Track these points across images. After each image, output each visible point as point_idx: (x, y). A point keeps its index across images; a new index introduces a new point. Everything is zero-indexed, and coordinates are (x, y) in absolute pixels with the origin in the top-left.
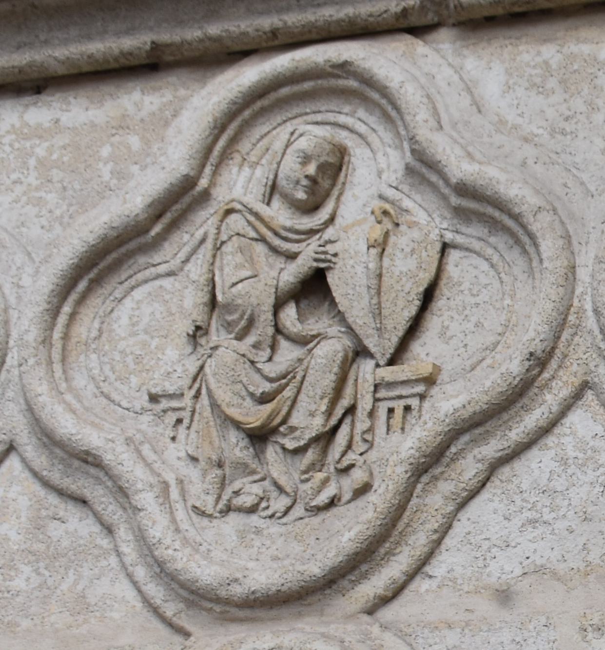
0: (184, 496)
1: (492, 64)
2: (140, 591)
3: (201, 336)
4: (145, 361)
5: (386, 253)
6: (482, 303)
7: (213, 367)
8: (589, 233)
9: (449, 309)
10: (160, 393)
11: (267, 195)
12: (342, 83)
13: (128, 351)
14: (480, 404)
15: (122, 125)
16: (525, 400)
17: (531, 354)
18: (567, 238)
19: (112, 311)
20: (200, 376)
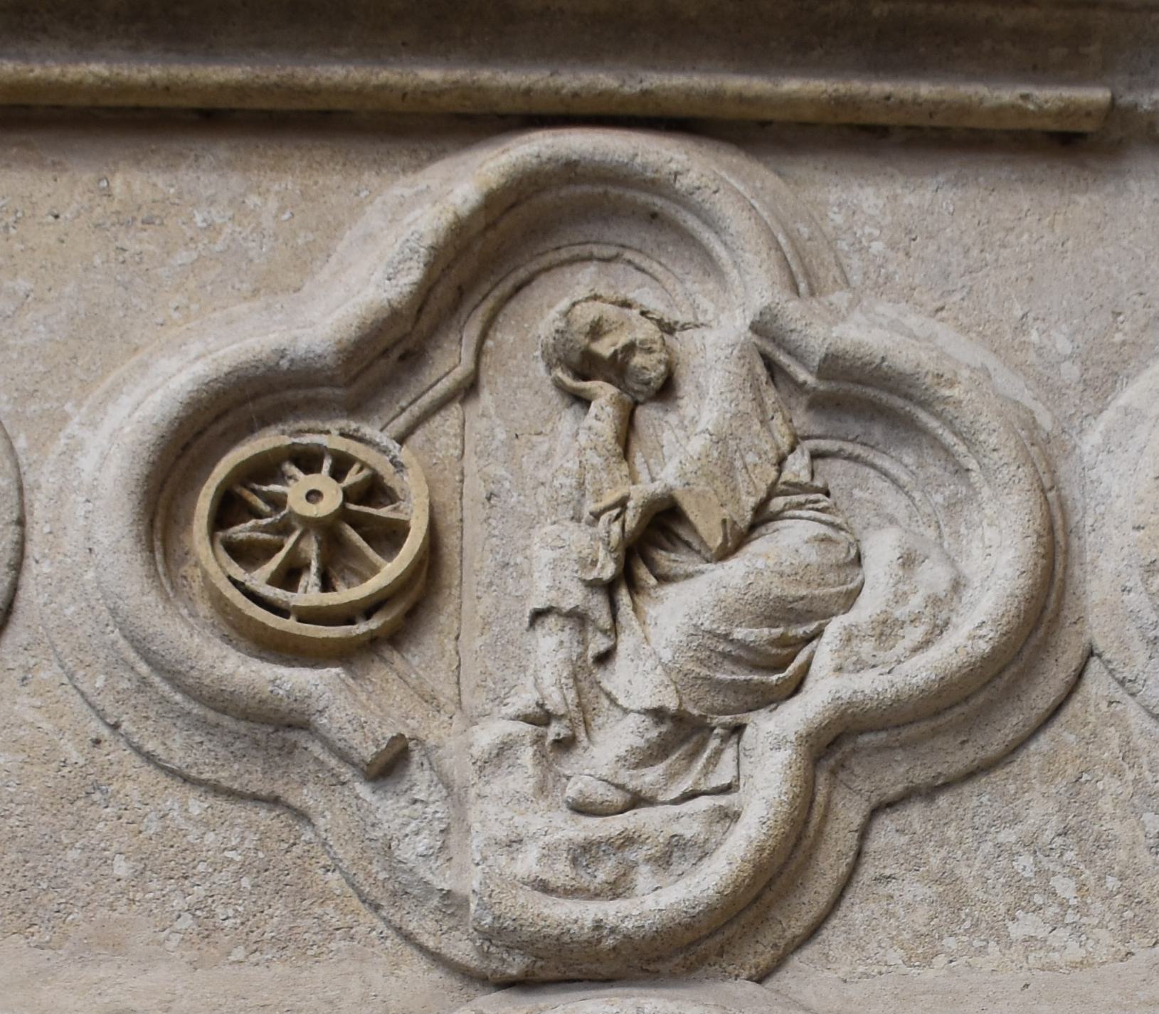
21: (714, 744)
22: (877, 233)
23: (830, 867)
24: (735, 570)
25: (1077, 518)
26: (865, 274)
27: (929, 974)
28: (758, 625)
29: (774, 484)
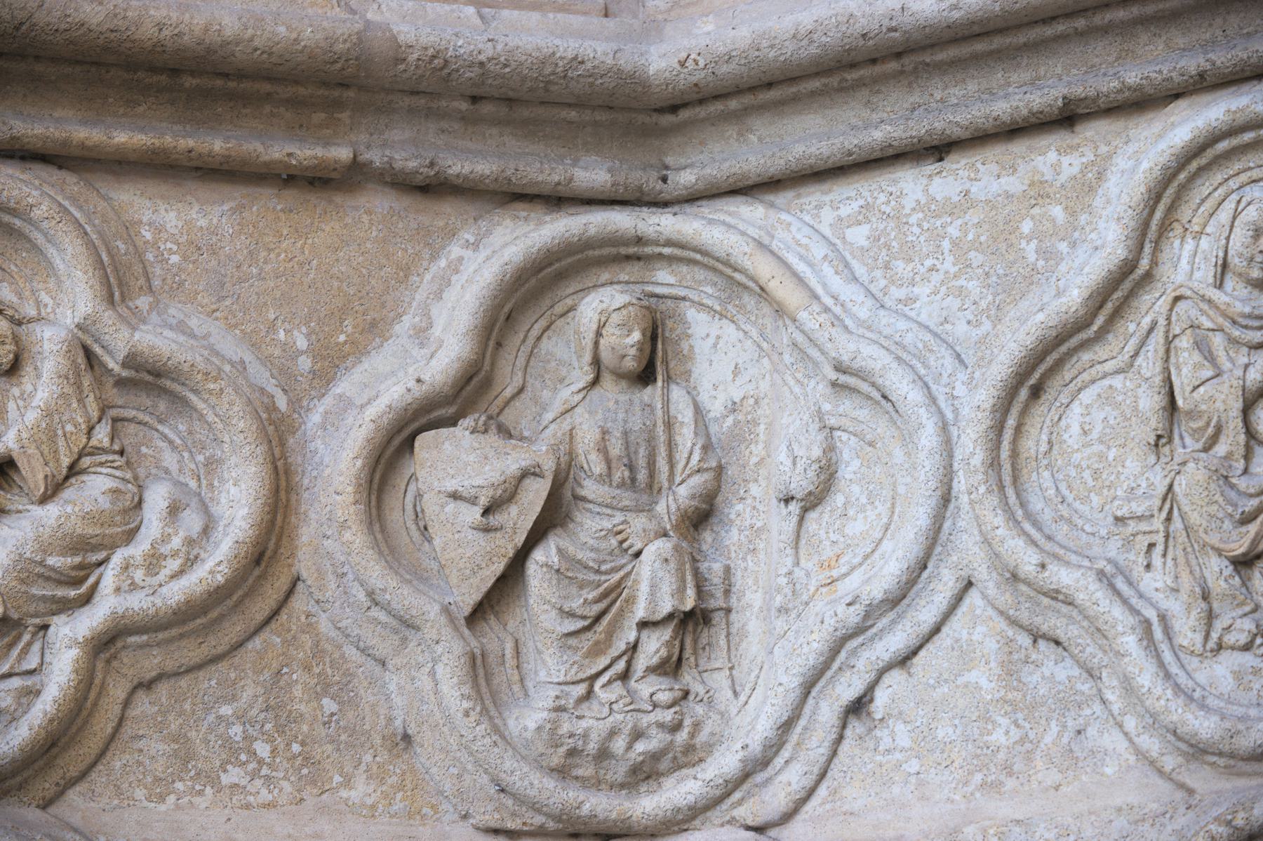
0: (1168, 634)
2: (1131, 741)
3: (1164, 445)
4: (1104, 476)
7: (1184, 486)
10: (1127, 516)
11: (1218, 276)
13: (1084, 465)
15: (1039, 192)
19: (1060, 419)
20: (1170, 496)
21: (26, 637)
22: (175, 248)
23: (103, 724)
24: (51, 512)
25: (297, 479)
26: (164, 280)
27: (162, 808)
28: (63, 555)
29: (84, 448)
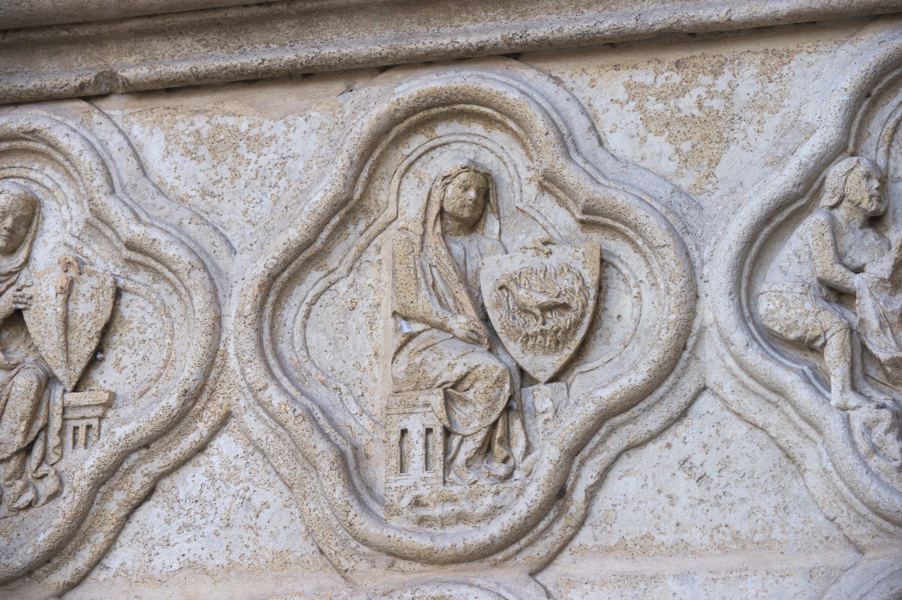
1: (154, 131)
5: (71, 298)
6: (147, 340)
8: (232, 286)
9: (122, 343)
12: (31, 145)
14: (146, 431)
16: (181, 426)
17: (186, 391)
18: (215, 292)
